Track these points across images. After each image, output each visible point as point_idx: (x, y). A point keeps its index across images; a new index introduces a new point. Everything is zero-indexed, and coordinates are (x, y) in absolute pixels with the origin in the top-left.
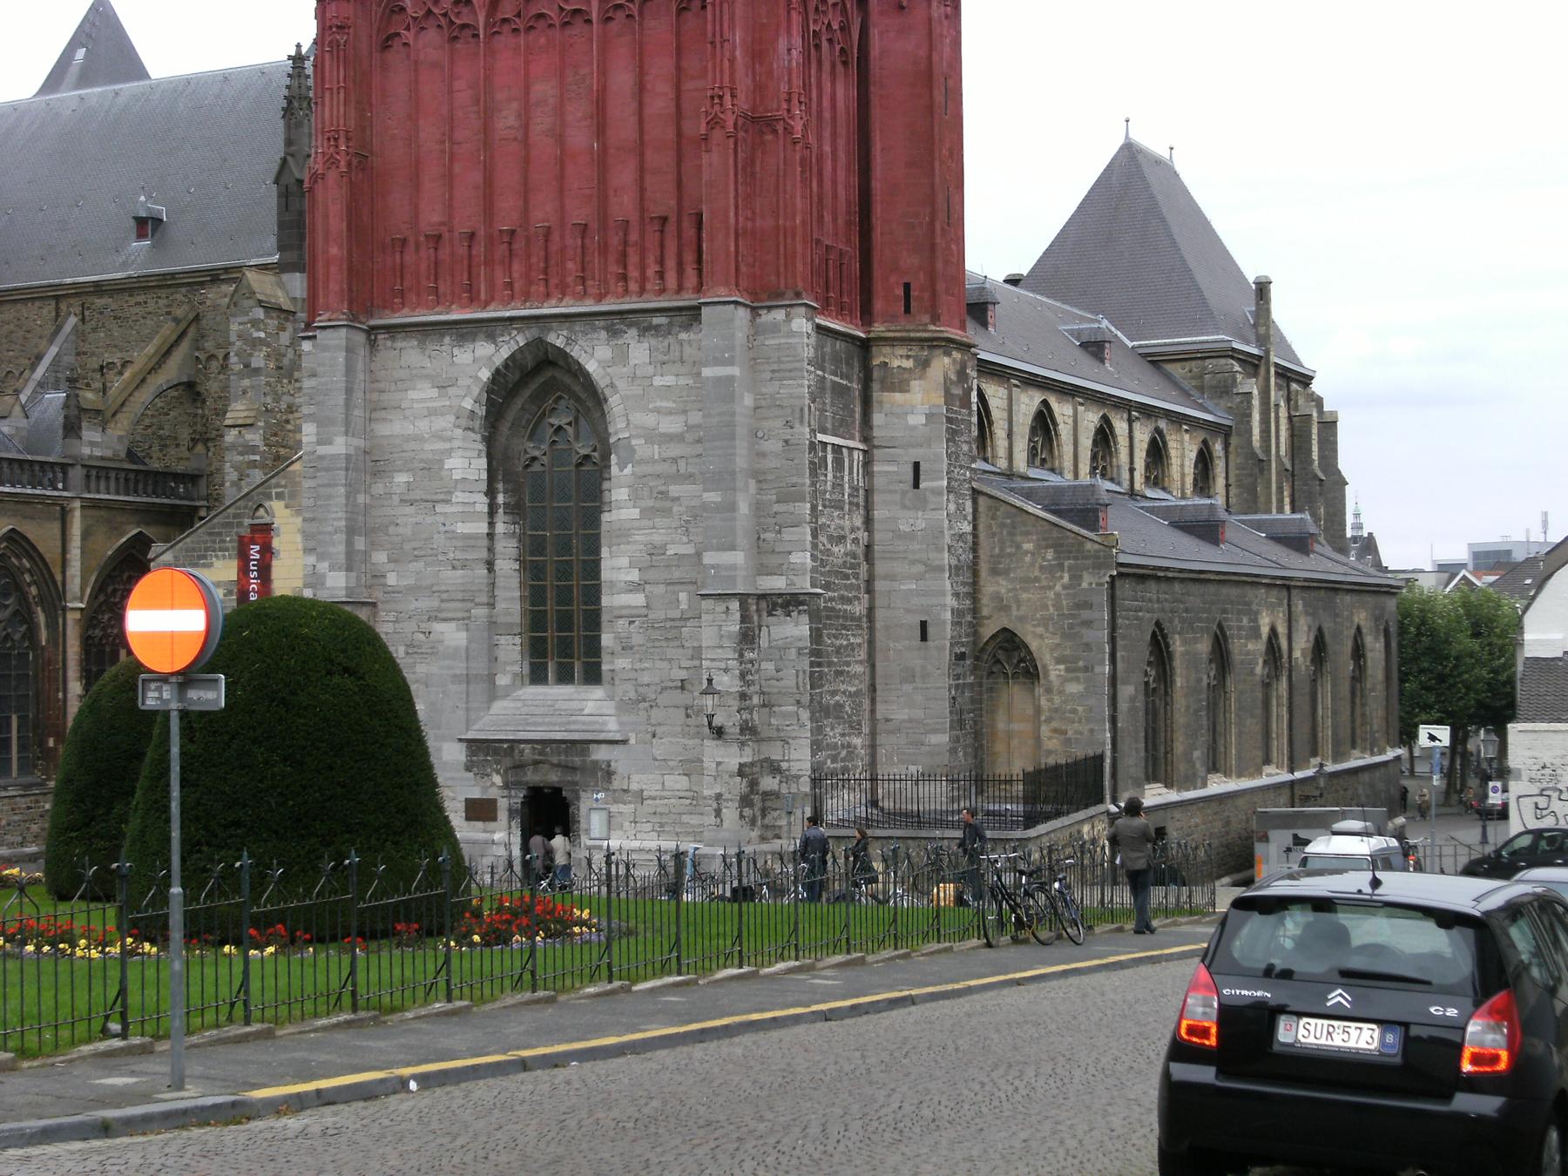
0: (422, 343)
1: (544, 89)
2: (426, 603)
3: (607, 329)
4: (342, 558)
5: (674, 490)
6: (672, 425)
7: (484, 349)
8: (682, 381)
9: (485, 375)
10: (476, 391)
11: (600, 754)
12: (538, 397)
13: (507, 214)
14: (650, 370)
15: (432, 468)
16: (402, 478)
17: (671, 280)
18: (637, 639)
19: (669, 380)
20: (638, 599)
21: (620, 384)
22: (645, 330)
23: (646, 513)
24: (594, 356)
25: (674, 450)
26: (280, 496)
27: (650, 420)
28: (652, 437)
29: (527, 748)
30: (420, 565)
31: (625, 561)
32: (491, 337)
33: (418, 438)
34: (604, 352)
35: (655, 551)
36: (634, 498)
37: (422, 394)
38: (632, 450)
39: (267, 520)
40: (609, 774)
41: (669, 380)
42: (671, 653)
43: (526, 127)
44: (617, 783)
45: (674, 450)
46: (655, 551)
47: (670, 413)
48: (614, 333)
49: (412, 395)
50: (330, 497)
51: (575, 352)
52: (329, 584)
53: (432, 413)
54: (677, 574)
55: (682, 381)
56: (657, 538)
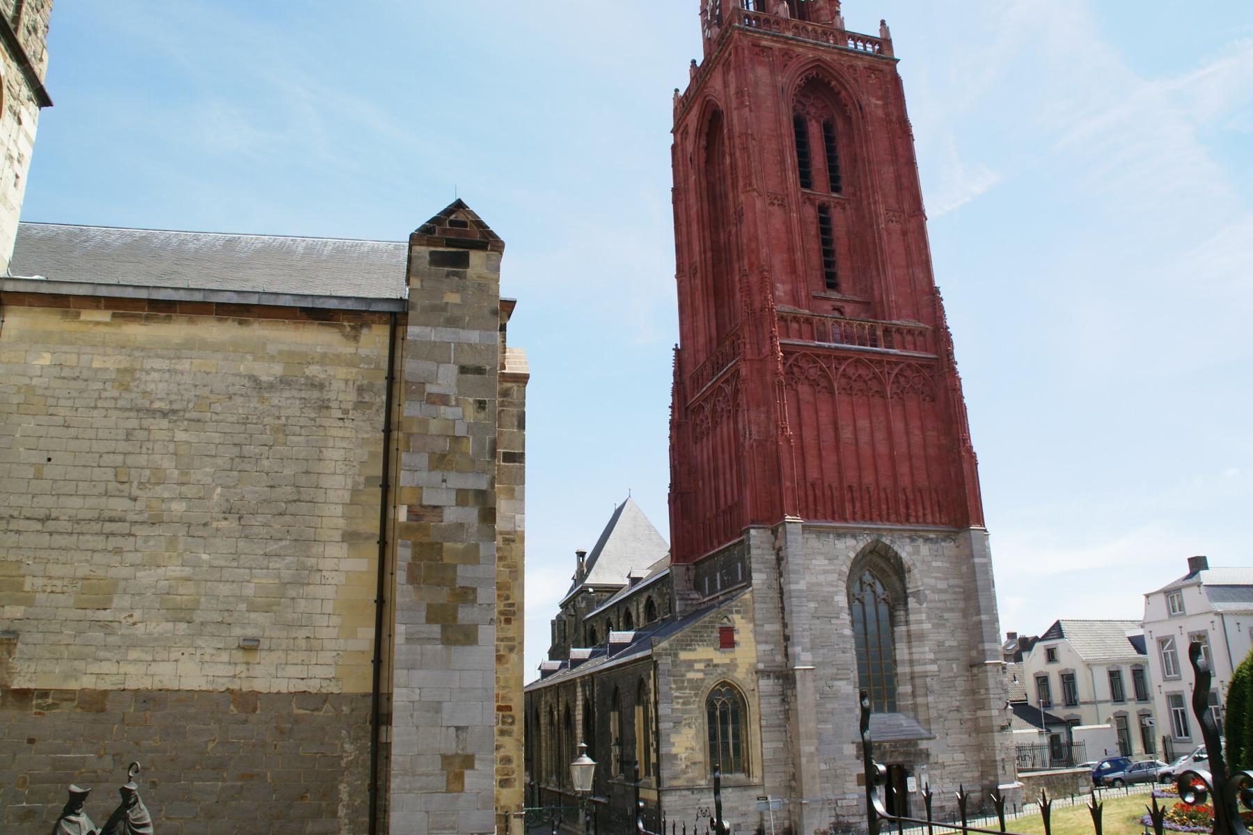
0: (818, 537)
1: (863, 423)
2: (830, 671)
3: (910, 537)
4: (808, 645)
5: (946, 615)
6: (942, 585)
7: (851, 542)
8: (945, 565)
9: (852, 555)
10: (849, 564)
11: (923, 745)
12: (862, 569)
13: (851, 476)
14: (930, 559)
15: (827, 600)
16: (812, 605)
17: (929, 518)
18: (936, 687)
19: (939, 564)
20: (933, 668)
21: (918, 564)
22: (927, 540)
23: (935, 626)
24: (905, 551)
25: (944, 597)
26: (738, 612)
27: (932, 582)
28: (935, 590)
29: (887, 745)
30: (825, 651)
31: (927, 649)
32: (854, 536)
33: (820, 584)
34: (909, 548)
35: (940, 644)
36: (929, 618)
37: (820, 562)
38: (926, 596)
39: (729, 625)
40: (928, 755)
41: (939, 564)
42: (951, 693)
43: (856, 439)
44: (932, 760)
45: (944, 597)
46: (940, 644)
47: (940, 579)
48: (912, 540)
49: (814, 562)
50: (799, 612)
51: (896, 548)
52: (802, 658)
53: (826, 572)
54: (951, 655)
55: (945, 565)
56: (940, 638)
